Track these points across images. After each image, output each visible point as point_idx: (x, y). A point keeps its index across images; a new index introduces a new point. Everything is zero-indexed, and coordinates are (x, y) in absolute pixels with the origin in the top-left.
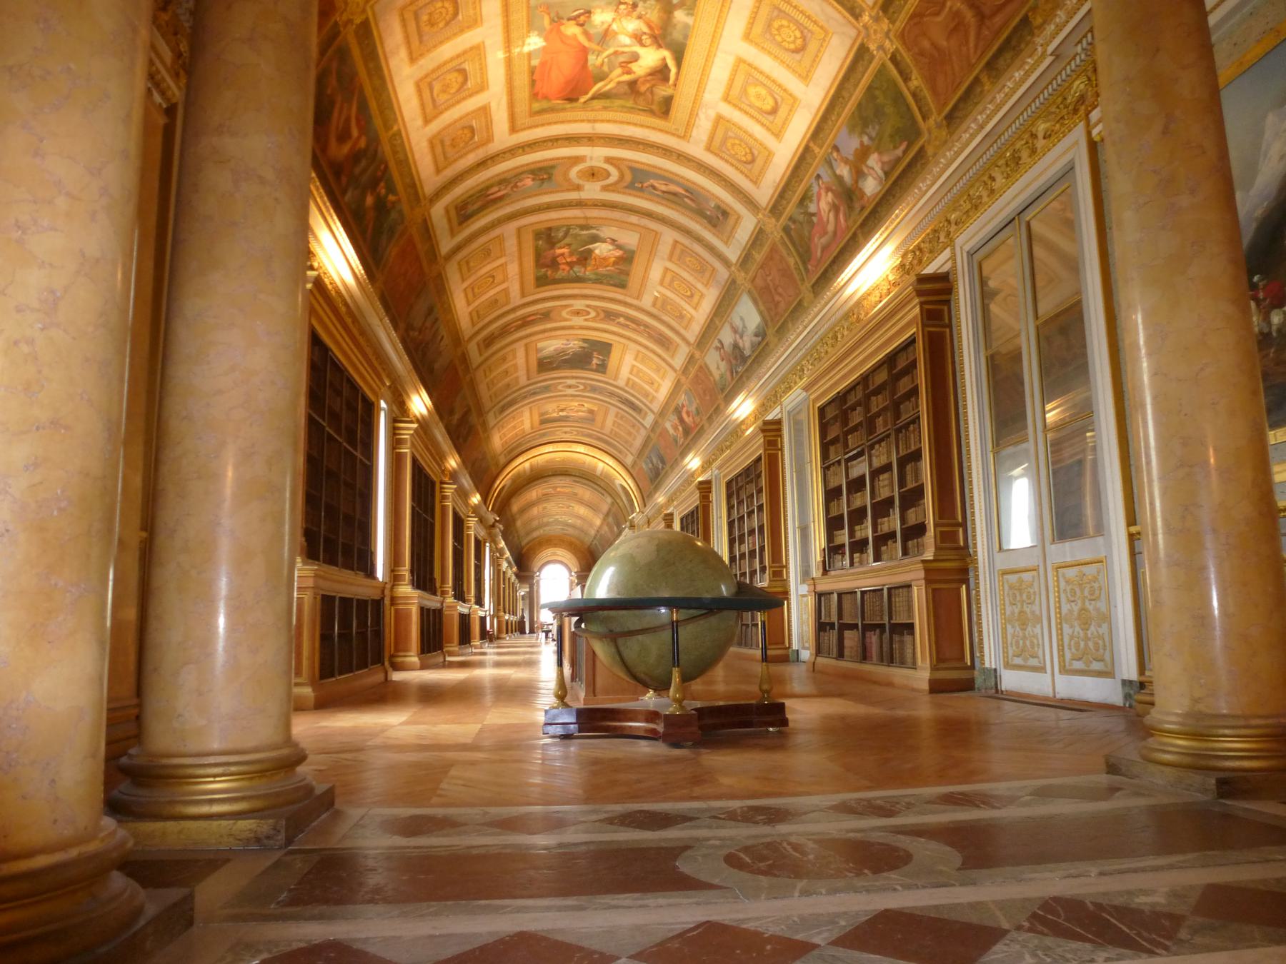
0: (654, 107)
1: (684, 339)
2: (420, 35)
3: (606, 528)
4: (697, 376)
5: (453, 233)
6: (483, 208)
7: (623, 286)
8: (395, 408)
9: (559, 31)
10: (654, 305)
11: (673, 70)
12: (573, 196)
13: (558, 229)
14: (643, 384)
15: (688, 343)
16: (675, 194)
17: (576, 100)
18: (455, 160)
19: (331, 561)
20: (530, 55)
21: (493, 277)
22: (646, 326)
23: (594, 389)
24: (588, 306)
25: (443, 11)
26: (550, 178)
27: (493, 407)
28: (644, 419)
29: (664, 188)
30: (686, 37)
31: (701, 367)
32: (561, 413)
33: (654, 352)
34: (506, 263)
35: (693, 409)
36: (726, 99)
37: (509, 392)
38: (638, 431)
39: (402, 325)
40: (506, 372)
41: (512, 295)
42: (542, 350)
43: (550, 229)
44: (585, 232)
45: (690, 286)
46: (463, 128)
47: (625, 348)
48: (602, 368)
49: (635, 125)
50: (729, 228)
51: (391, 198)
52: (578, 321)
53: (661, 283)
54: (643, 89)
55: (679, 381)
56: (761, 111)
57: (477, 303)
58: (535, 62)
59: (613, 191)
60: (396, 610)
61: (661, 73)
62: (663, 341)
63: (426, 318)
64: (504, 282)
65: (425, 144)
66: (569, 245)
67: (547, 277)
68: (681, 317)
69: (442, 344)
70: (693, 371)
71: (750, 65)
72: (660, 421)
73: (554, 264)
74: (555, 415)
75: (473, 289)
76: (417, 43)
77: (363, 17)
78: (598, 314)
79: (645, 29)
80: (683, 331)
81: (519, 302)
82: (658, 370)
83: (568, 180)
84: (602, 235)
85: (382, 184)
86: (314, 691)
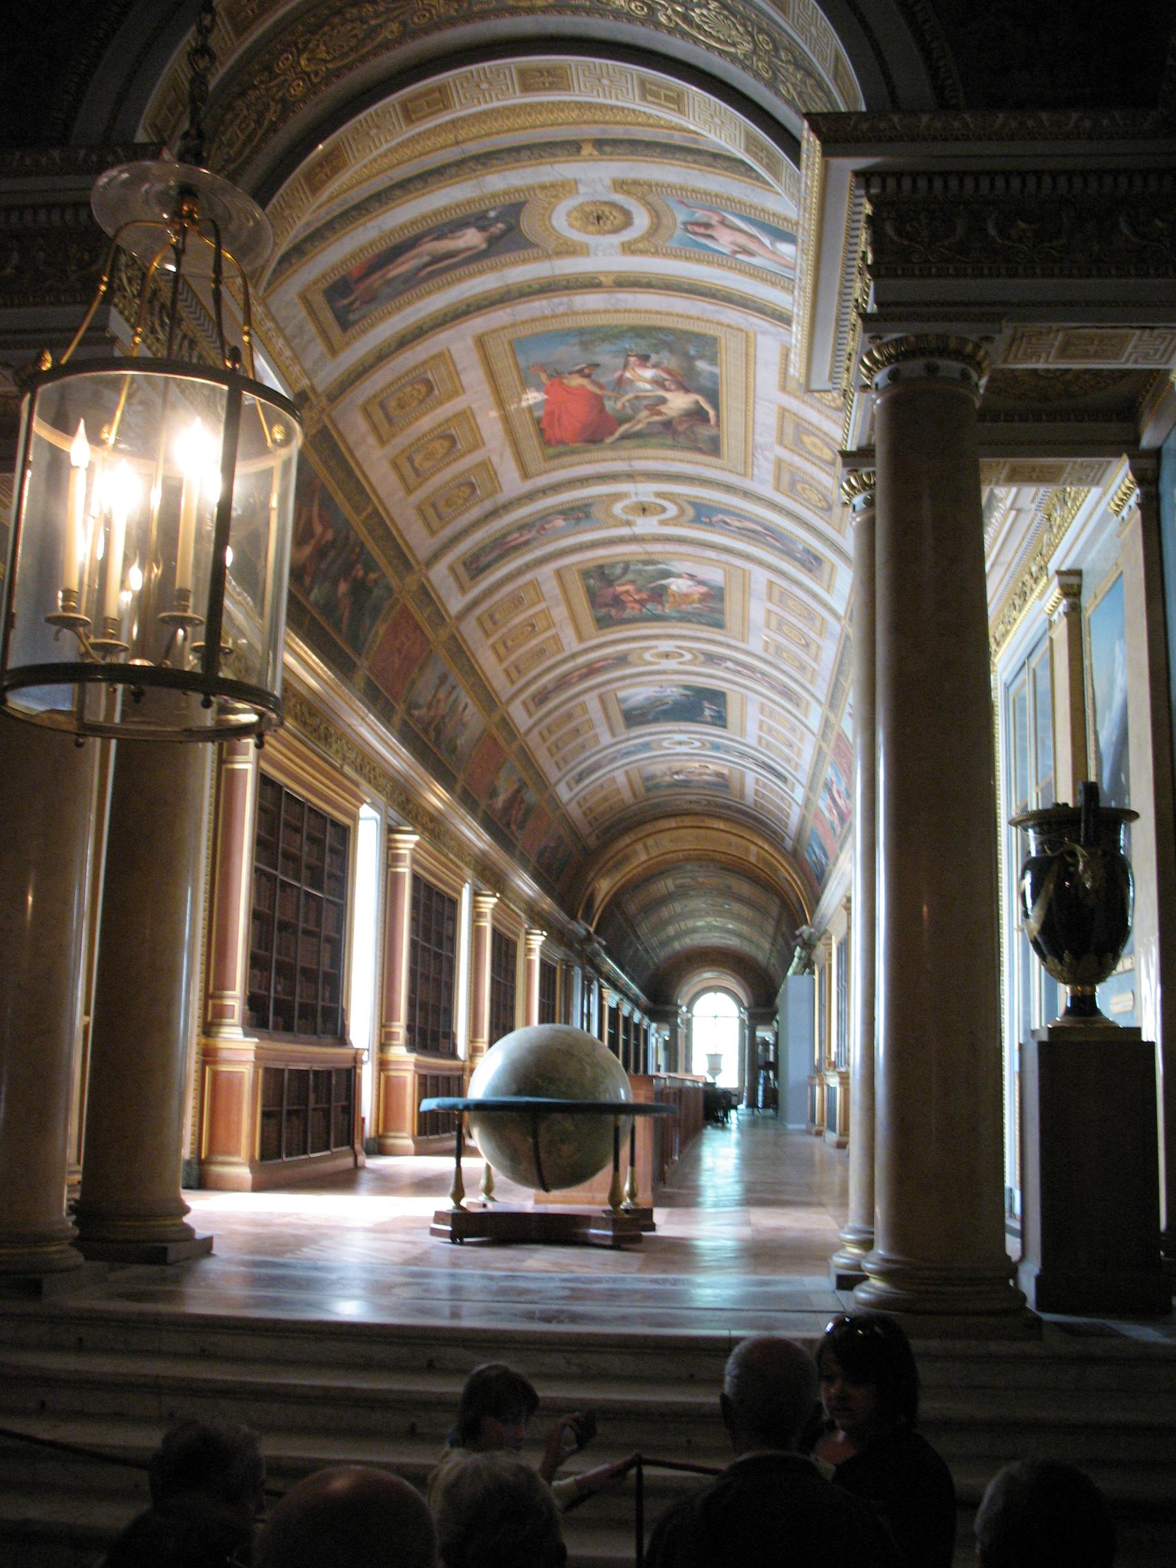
0: (701, 445)
1: (813, 695)
2: (389, 419)
3: (780, 940)
4: (838, 746)
5: (463, 590)
6: (501, 557)
7: (719, 625)
8: (392, 813)
9: (561, 384)
10: (766, 650)
11: (712, 413)
12: (625, 531)
13: (613, 566)
14: (778, 744)
15: (818, 700)
16: (754, 531)
17: (601, 441)
18: (454, 518)
19: (288, 1027)
20: (530, 409)
21: (533, 626)
22: (763, 674)
23: (716, 747)
24: (679, 647)
25: (415, 393)
26: (588, 516)
27: (564, 776)
28: (793, 791)
29: (738, 524)
30: (716, 383)
31: (839, 735)
32: (676, 777)
33: (783, 708)
34: (548, 608)
35: (842, 789)
36: (781, 442)
37: (588, 753)
38: (790, 807)
39: (401, 708)
40: (577, 731)
41: (565, 642)
42: (625, 700)
43: (601, 567)
44: (650, 568)
45: (803, 635)
46: (459, 486)
47: (743, 701)
48: (720, 720)
49: (681, 461)
50: (826, 577)
51: (372, 576)
52: (671, 664)
53: (768, 626)
54: (681, 428)
55: (820, 748)
56: (821, 459)
57: (513, 657)
58: (539, 413)
59: (676, 525)
60: (388, 1079)
61: (697, 415)
62: (787, 693)
63: (438, 687)
64: (549, 628)
65: (411, 514)
66: (633, 582)
67: (611, 617)
68: (802, 668)
69: (467, 712)
70: (832, 737)
71: (795, 414)
72: (811, 796)
73: (617, 601)
74: (668, 779)
75: (505, 644)
76: (386, 424)
77: (320, 426)
78: (696, 657)
79: (665, 376)
80: (808, 686)
81: (576, 647)
82: (793, 730)
83: (614, 516)
84: (674, 570)
85: (359, 566)
86: (252, 1172)
